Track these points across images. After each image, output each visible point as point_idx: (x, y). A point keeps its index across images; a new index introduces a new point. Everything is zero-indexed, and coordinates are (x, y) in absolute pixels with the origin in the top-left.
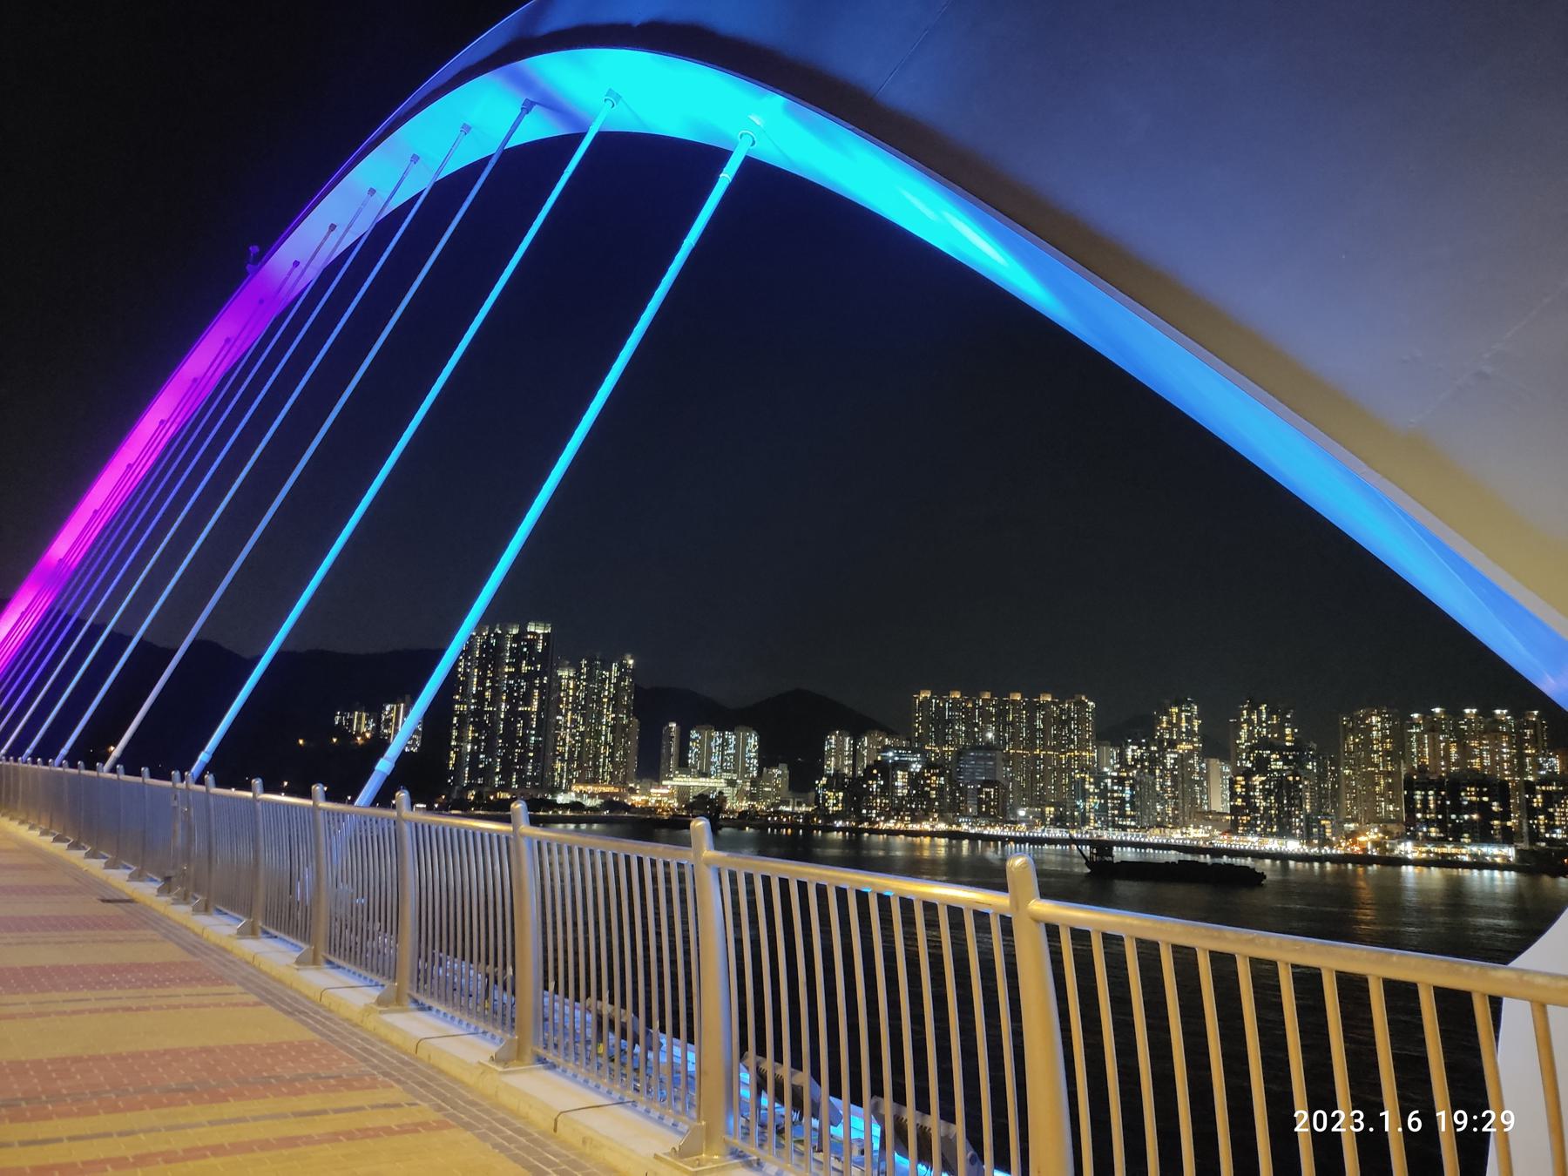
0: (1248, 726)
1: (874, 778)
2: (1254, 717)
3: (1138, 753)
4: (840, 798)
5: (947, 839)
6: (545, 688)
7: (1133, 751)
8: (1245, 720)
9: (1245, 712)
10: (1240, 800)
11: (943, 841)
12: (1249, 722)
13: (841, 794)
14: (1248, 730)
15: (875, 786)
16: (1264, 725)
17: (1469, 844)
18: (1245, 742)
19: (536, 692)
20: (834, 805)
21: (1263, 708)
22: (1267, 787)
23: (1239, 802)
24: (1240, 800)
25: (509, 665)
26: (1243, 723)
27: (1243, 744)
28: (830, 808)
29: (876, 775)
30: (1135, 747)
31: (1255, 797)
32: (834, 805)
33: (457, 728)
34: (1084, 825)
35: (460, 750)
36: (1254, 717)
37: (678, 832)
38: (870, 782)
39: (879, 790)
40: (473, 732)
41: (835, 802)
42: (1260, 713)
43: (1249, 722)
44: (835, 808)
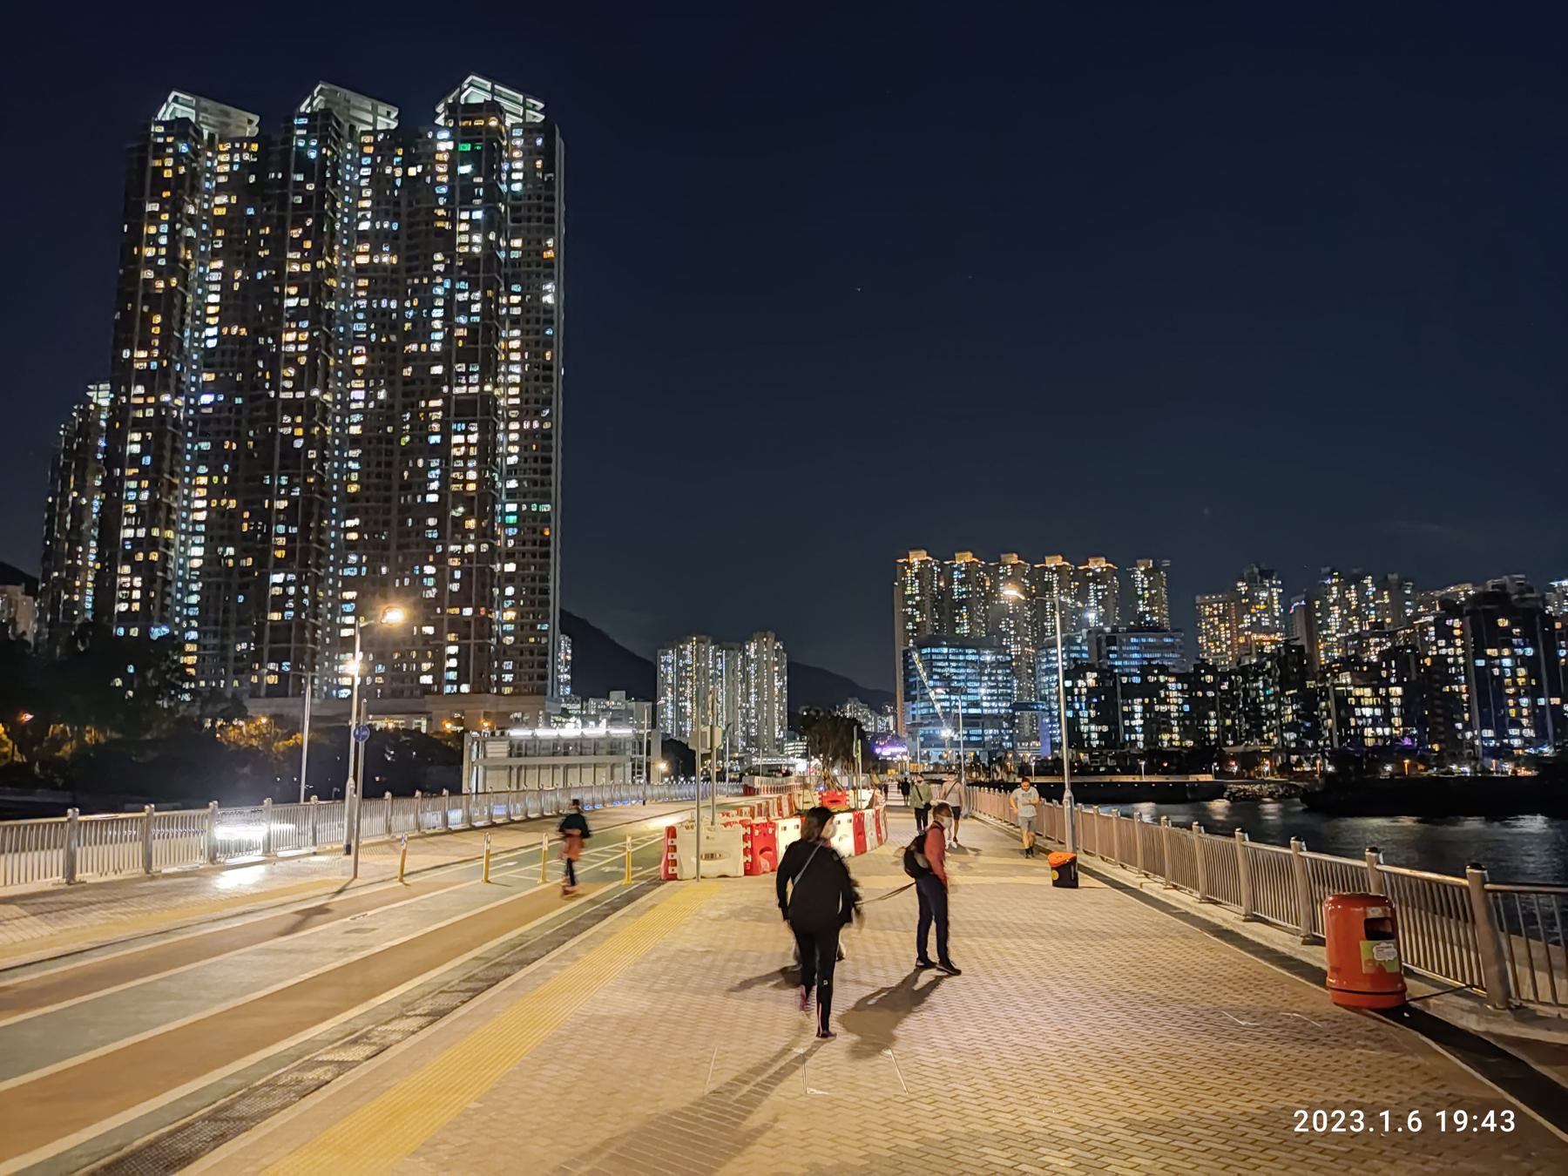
5: (1151, 804)
6: (550, 322)
9: (1334, 589)
12: (1342, 602)
14: (1341, 615)
16: (1372, 605)
18: (1338, 631)
19: (513, 339)
20: (1375, 722)
21: (1368, 581)
25: (376, 239)
26: (1333, 605)
27: (1334, 635)
28: (1369, 731)
32: (1375, 722)
33: (144, 473)
34: (882, 773)
35: (165, 558)
36: (1352, 595)
37: (1335, 822)
40: (213, 492)
42: (1362, 590)
43: (1342, 602)
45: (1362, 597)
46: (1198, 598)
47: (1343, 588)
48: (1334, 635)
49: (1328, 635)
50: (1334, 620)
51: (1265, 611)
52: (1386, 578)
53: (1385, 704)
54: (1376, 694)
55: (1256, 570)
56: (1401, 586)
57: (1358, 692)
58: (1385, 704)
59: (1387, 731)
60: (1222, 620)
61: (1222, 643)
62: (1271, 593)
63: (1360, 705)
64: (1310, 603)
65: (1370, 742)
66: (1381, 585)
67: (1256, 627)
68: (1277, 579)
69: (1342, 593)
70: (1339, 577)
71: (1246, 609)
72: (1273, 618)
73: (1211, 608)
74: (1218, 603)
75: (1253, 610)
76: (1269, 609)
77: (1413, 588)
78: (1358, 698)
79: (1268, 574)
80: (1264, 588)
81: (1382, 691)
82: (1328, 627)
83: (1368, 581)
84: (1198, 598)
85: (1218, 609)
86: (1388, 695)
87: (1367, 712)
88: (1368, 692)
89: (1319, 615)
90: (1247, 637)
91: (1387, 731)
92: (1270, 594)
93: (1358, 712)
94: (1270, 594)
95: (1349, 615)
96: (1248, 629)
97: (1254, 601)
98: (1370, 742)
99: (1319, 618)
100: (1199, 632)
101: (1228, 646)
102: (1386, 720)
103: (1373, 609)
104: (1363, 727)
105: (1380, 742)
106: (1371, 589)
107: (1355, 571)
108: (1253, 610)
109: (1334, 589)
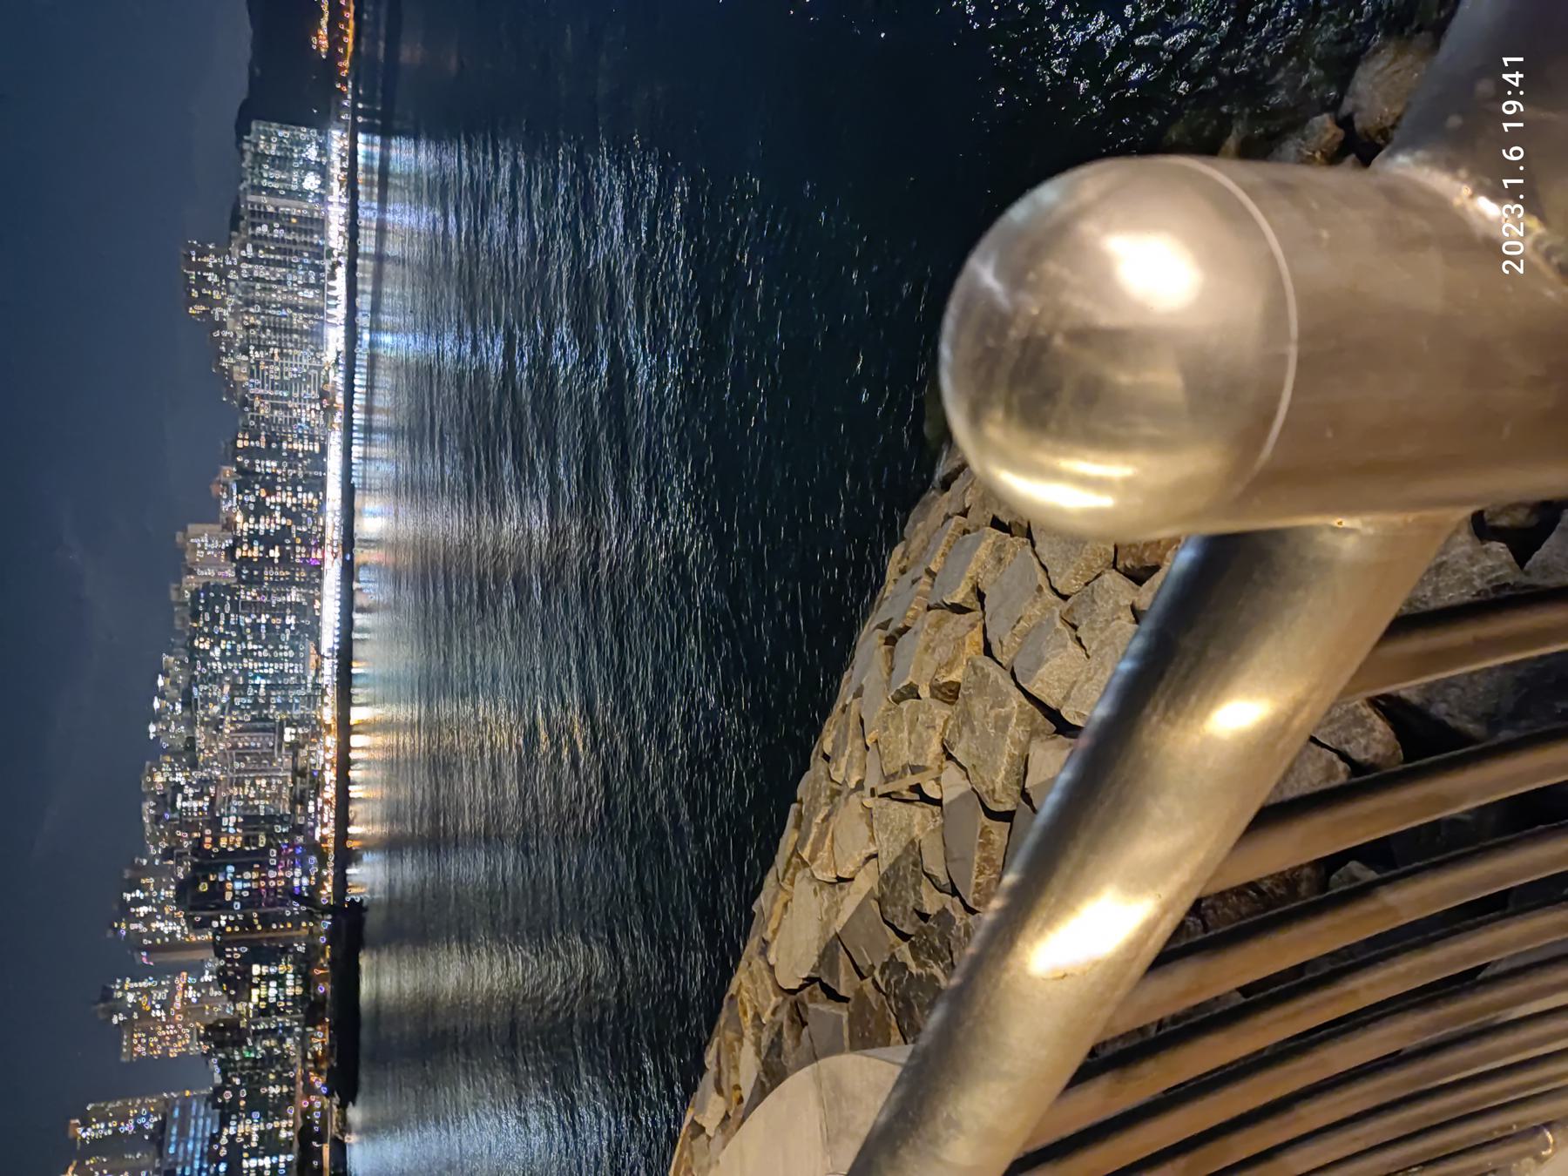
0: (155, 920)
1: (218, 889)
2: (143, 910)
3: (190, 791)
4: (265, 970)
7: (185, 799)
8: (147, 925)
10: (272, 553)
11: (357, 715)
12: (149, 918)
13: (256, 969)
14: (162, 921)
15: (238, 885)
17: (323, 552)
18: (179, 924)
20: (282, 984)
21: (128, 897)
22: (252, 507)
23: (275, 553)
24: (272, 553)
26: (150, 928)
28: (290, 992)
29: (211, 884)
30: (179, 797)
31: (267, 531)
32: (282, 984)
36: (143, 910)
38: (228, 896)
39: (247, 875)
41: (273, 984)
42: (138, 902)
44: (289, 983)
45: (145, 902)
46: (124, 1059)
47: (135, 918)
48: (183, 928)
49: (182, 934)
50: (166, 927)
51: (150, 996)
52: (130, 880)
53: (266, 978)
54: (257, 986)
55: (102, 1005)
56: (140, 867)
57: (255, 999)
58: (266, 978)
59: (290, 976)
60: (154, 1034)
61: (180, 1033)
62: (131, 990)
63: (266, 999)
64: (147, 949)
65: (299, 991)
66: (134, 885)
67: (166, 1005)
68: (115, 983)
69: (137, 920)
70: (120, 922)
71: (145, 1015)
72: (160, 987)
73: (138, 1046)
74: (132, 1037)
75: (148, 1008)
76: (147, 992)
77: (142, 857)
78: (260, 999)
79: (107, 995)
80: (123, 998)
81: (255, 981)
82: (174, 932)
83: (128, 897)
84: (124, 1059)
85: (139, 1039)
86: (260, 976)
87: (273, 992)
88: (255, 992)
89: (159, 941)
90: (177, 1012)
91: (290, 976)
92: (128, 993)
93: (273, 1000)
94: (128, 993)
95: (163, 914)
96: (167, 1012)
97: (137, 1006)
98: (299, 991)
99: (163, 940)
100: (164, 1057)
101: (185, 1027)
102: (280, 979)
103: (159, 891)
104: (285, 996)
105: (299, 982)
106: (138, 893)
107: (116, 907)
108: (148, 1008)
109: (133, 926)
